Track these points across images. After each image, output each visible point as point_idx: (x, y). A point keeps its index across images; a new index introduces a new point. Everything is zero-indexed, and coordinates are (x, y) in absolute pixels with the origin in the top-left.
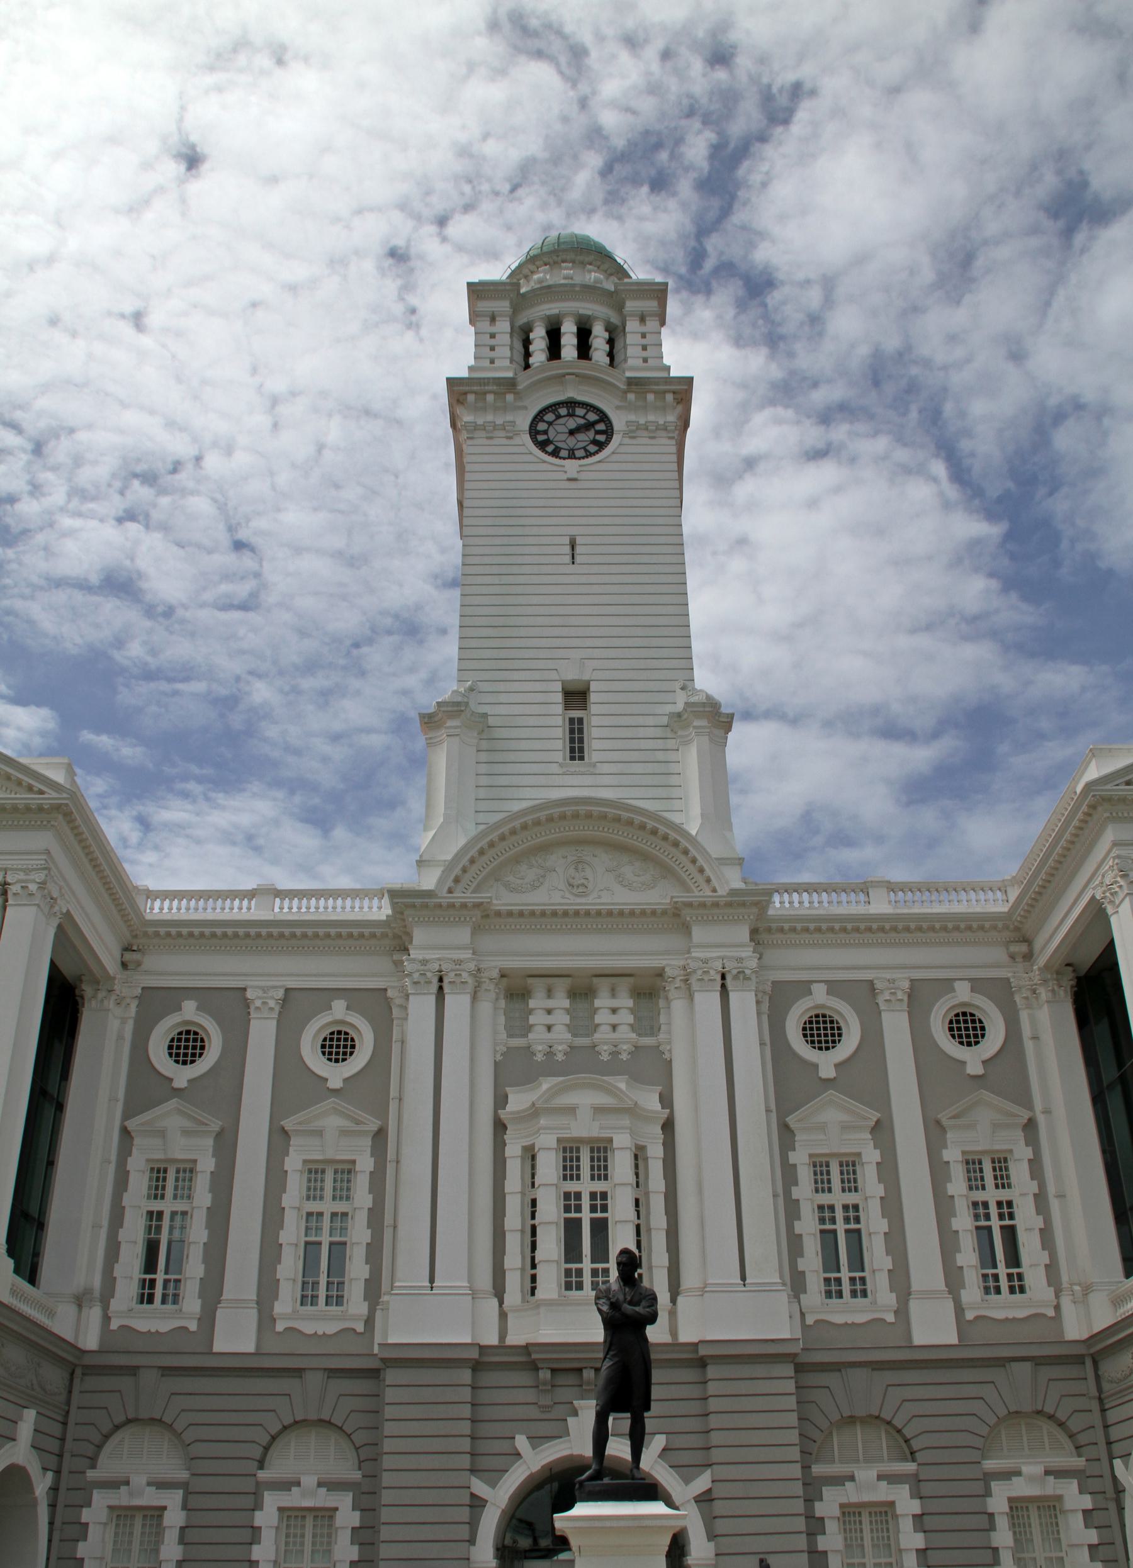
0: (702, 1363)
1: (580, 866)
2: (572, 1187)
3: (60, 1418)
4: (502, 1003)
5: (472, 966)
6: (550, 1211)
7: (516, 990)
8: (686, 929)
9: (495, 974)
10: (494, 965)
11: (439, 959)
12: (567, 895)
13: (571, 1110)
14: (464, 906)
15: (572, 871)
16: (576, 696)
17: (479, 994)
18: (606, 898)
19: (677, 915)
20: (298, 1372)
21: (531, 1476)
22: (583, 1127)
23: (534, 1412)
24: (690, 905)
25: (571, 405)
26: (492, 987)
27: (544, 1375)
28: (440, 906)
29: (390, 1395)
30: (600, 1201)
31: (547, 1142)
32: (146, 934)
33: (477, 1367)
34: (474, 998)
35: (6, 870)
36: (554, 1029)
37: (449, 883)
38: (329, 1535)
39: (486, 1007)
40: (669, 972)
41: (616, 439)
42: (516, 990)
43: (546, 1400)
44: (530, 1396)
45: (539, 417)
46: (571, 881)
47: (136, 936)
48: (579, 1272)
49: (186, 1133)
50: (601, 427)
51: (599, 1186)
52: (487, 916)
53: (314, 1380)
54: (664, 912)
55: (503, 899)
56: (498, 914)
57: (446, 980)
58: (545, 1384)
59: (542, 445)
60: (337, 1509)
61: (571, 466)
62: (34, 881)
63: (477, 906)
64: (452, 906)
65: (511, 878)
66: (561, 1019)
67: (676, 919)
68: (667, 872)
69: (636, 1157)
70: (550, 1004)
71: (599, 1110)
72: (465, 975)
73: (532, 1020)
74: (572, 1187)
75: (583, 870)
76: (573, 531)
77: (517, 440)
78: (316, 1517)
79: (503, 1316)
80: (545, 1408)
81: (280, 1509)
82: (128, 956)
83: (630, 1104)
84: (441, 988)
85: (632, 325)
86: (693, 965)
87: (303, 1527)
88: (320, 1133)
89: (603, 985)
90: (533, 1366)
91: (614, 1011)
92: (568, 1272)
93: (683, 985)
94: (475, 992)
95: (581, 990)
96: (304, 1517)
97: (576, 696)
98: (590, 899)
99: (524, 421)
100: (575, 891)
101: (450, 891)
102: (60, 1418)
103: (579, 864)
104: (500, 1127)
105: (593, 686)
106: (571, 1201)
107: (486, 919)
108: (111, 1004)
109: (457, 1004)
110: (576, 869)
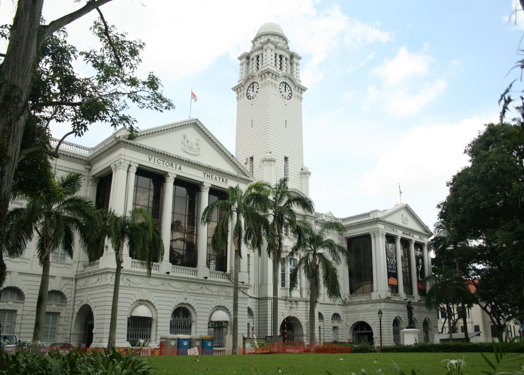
16: (286, 159)
23: (284, 308)
25: (286, 84)
41: (293, 97)
44: (284, 305)
45: (280, 85)
50: (290, 92)
59: (281, 92)
61: (286, 101)
76: (287, 119)
77: (277, 89)
80: (286, 308)
85: (295, 65)
97: (286, 159)
99: (278, 83)
105: (289, 159)
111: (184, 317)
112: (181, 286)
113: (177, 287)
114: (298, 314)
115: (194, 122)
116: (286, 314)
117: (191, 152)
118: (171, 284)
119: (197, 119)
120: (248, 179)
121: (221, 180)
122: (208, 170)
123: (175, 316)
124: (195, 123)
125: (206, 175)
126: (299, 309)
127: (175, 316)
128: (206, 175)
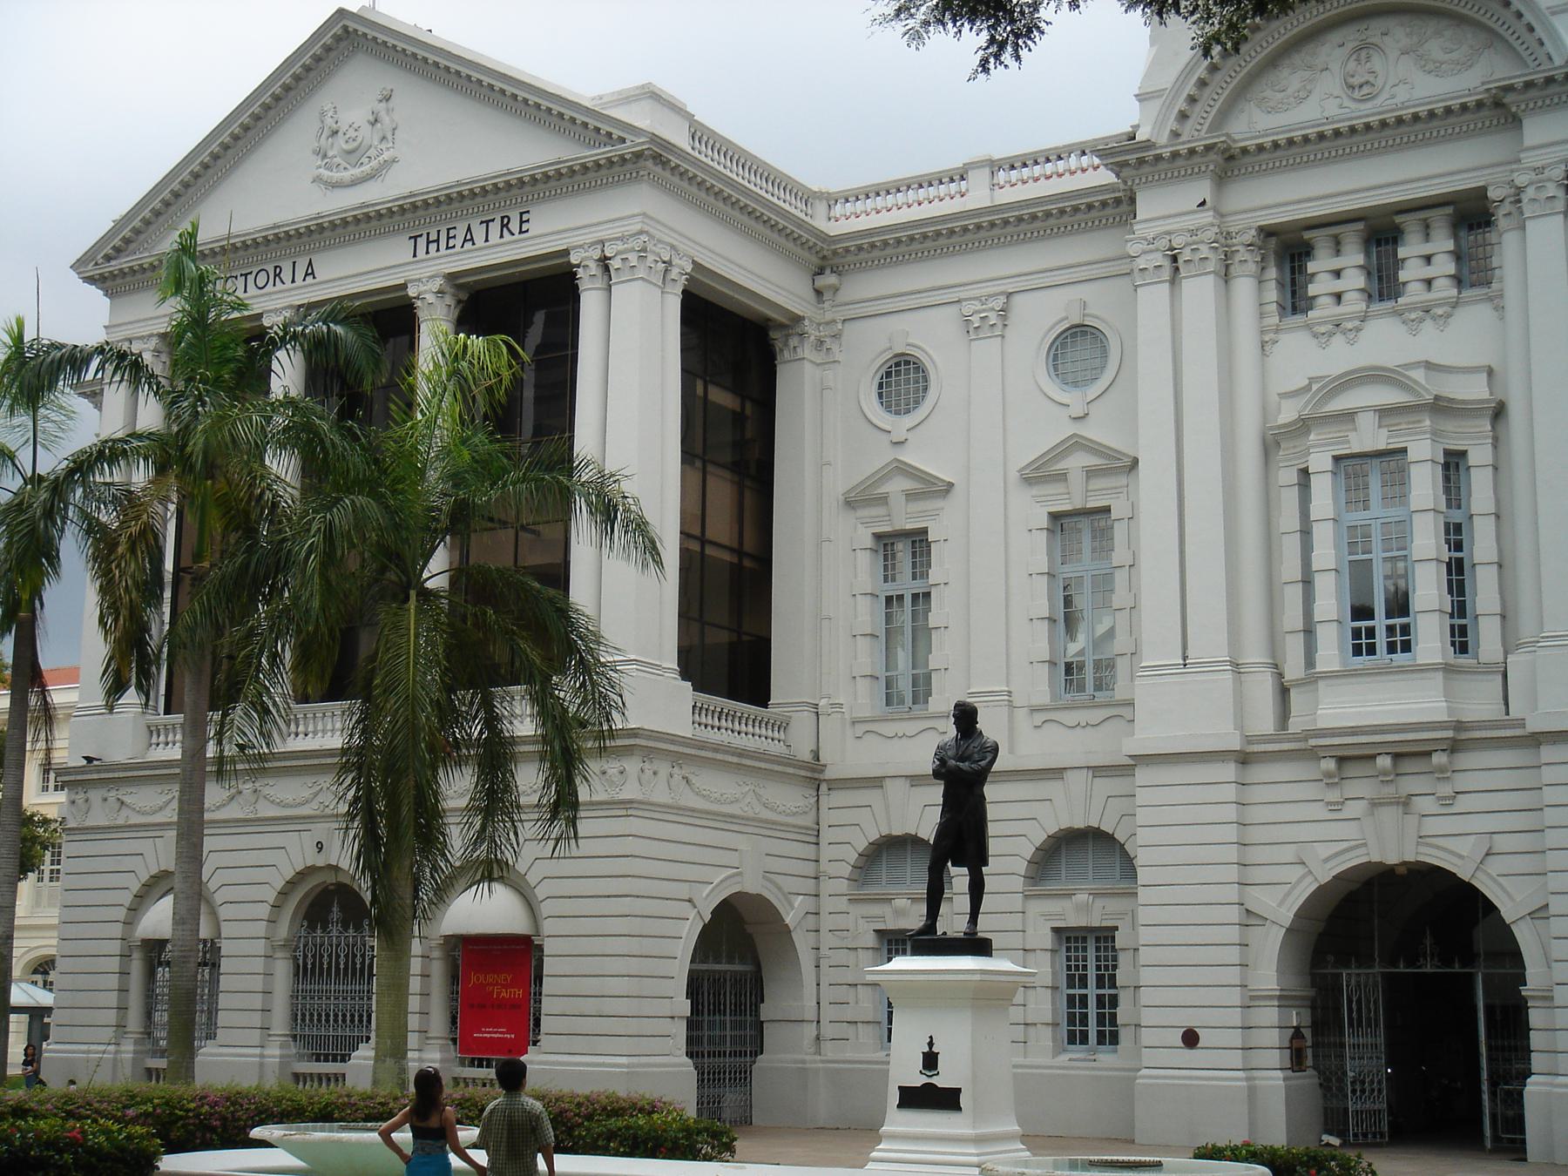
0: (1537, 740)
1: (1363, 54)
2: (1357, 517)
3: (813, 840)
4: (1272, 273)
5: (1210, 234)
6: (1325, 553)
7: (1289, 250)
8: (1515, 122)
9: (1250, 236)
10: (1245, 226)
11: (1169, 233)
12: (1347, 103)
13: (1349, 416)
14: (1192, 152)
15: (1352, 65)
17: (1232, 269)
18: (1402, 95)
19: (1498, 104)
20: (1056, 773)
21: (1321, 889)
22: (1369, 436)
23: (1319, 811)
24: (1509, 89)
26: (1247, 256)
27: (1331, 765)
28: (1159, 158)
29: (1142, 796)
30: (1399, 535)
31: (1320, 461)
32: (835, 252)
33: (1244, 759)
34: (1226, 276)
35: (602, 242)
36: (1345, 297)
37: (1171, 124)
38: (1115, 959)
39: (1244, 287)
40: (1492, 194)
42: (1289, 250)
43: (1333, 795)
46: (1351, 80)
47: (824, 258)
48: (1371, 632)
49: (911, 496)
51: (1394, 513)
52: (1231, 158)
53: (1077, 780)
54: (1480, 105)
55: (1254, 124)
56: (1244, 151)
57: (1180, 261)
58: (1328, 775)
60: (1116, 928)
62: (633, 250)
63: (1208, 148)
64: (1175, 155)
65: (1268, 93)
66: (1355, 280)
67: (1498, 111)
68: (1493, 37)
69: (1446, 466)
70: (1336, 263)
71: (1384, 412)
72: (1205, 251)
73: (1312, 290)
74: (1357, 517)
75: (1368, 58)
78: (1098, 940)
79: (1284, 692)
81: (1056, 930)
82: (822, 281)
83: (1429, 398)
84: (1177, 269)
86: (1521, 180)
87: (1085, 949)
88: (1062, 477)
89: (1410, 222)
90: (1313, 754)
91: (1428, 259)
92: (1356, 634)
93: (1512, 208)
94: (1227, 266)
95: (1381, 233)
96: (1084, 939)
98: (1378, 101)
100: (1357, 94)
101: (1176, 134)
102: (813, 840)
103: (1364, 49)
104: (1270, 445)
106: (1356, 539)
107: (1230, 163)
108: (807, 351)
109: (1200, 290)
110: (1358, 60)
111: (346, 928)
112: (307, 793)
113: (289, 798)
114: (1464, 846)
115: (337, 29)
116: (1324, 851)
117: (357, 172)
118: (266, 791)
119: (341, 13)
120: (621, 150)
121: (495, 228)
122: (420, 216)
123: (312, 927)
124: (345, 28)
125: (422, 242)
126: (1463, 803)
127: (312, 927)
128: (422, 242)
